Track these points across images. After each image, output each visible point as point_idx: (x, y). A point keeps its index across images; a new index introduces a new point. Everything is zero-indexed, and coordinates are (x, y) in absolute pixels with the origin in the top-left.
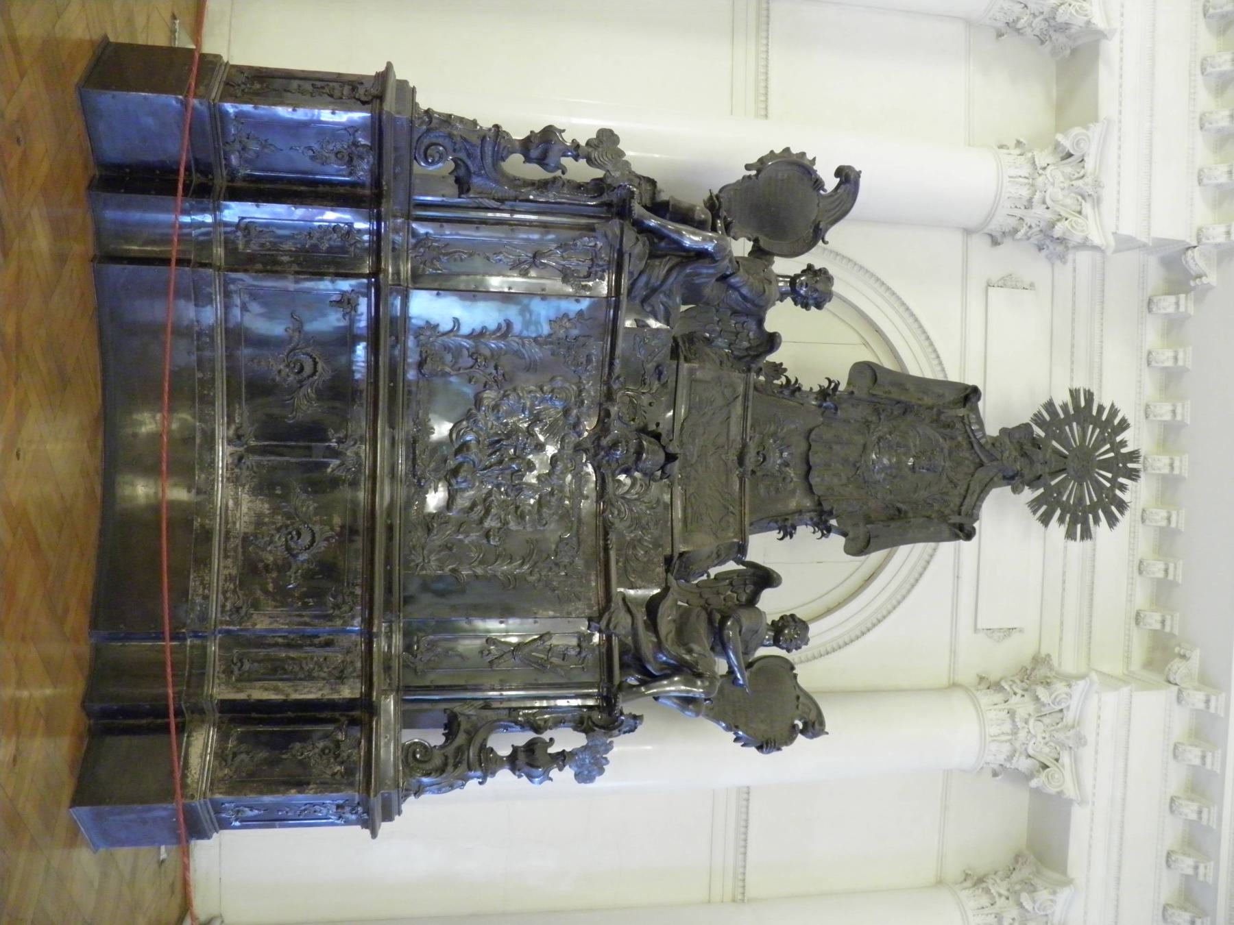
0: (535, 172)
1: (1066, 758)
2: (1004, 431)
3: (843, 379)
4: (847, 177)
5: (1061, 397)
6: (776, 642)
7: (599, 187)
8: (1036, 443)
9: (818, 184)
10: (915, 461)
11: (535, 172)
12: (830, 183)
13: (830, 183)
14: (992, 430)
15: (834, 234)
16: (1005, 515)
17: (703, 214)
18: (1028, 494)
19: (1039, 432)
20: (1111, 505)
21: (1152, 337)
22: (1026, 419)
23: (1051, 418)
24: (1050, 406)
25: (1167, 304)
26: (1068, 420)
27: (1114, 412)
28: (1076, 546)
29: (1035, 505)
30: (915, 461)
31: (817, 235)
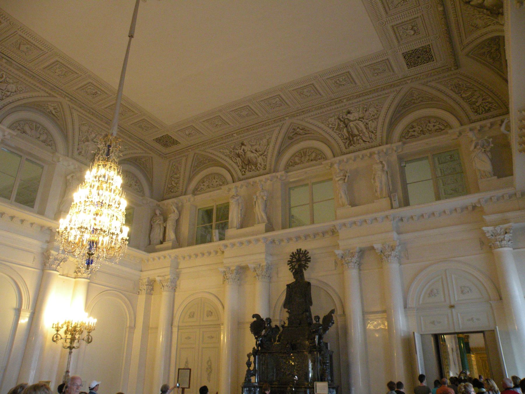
0: (253, 365)
2: (294, 278)
3: (286, 310)
4: (254, 316)
6: (319, 321)
7: (255, 357)
8: (295, 271)
9: (255, 321)
11: (253, 365)
12: (255, 319)
13: (255, 319)
14: (294, 280)
15: (262, 317)
20: (306, 253)
21: (283, 244)
22: (292, 274)
23: (292, 268)
24: (290, 269)
25: (277, 242)
26: (292, 265)
27: (291, 256)
29: (305, 269)
30: (299, 294)
31: (262, 320)
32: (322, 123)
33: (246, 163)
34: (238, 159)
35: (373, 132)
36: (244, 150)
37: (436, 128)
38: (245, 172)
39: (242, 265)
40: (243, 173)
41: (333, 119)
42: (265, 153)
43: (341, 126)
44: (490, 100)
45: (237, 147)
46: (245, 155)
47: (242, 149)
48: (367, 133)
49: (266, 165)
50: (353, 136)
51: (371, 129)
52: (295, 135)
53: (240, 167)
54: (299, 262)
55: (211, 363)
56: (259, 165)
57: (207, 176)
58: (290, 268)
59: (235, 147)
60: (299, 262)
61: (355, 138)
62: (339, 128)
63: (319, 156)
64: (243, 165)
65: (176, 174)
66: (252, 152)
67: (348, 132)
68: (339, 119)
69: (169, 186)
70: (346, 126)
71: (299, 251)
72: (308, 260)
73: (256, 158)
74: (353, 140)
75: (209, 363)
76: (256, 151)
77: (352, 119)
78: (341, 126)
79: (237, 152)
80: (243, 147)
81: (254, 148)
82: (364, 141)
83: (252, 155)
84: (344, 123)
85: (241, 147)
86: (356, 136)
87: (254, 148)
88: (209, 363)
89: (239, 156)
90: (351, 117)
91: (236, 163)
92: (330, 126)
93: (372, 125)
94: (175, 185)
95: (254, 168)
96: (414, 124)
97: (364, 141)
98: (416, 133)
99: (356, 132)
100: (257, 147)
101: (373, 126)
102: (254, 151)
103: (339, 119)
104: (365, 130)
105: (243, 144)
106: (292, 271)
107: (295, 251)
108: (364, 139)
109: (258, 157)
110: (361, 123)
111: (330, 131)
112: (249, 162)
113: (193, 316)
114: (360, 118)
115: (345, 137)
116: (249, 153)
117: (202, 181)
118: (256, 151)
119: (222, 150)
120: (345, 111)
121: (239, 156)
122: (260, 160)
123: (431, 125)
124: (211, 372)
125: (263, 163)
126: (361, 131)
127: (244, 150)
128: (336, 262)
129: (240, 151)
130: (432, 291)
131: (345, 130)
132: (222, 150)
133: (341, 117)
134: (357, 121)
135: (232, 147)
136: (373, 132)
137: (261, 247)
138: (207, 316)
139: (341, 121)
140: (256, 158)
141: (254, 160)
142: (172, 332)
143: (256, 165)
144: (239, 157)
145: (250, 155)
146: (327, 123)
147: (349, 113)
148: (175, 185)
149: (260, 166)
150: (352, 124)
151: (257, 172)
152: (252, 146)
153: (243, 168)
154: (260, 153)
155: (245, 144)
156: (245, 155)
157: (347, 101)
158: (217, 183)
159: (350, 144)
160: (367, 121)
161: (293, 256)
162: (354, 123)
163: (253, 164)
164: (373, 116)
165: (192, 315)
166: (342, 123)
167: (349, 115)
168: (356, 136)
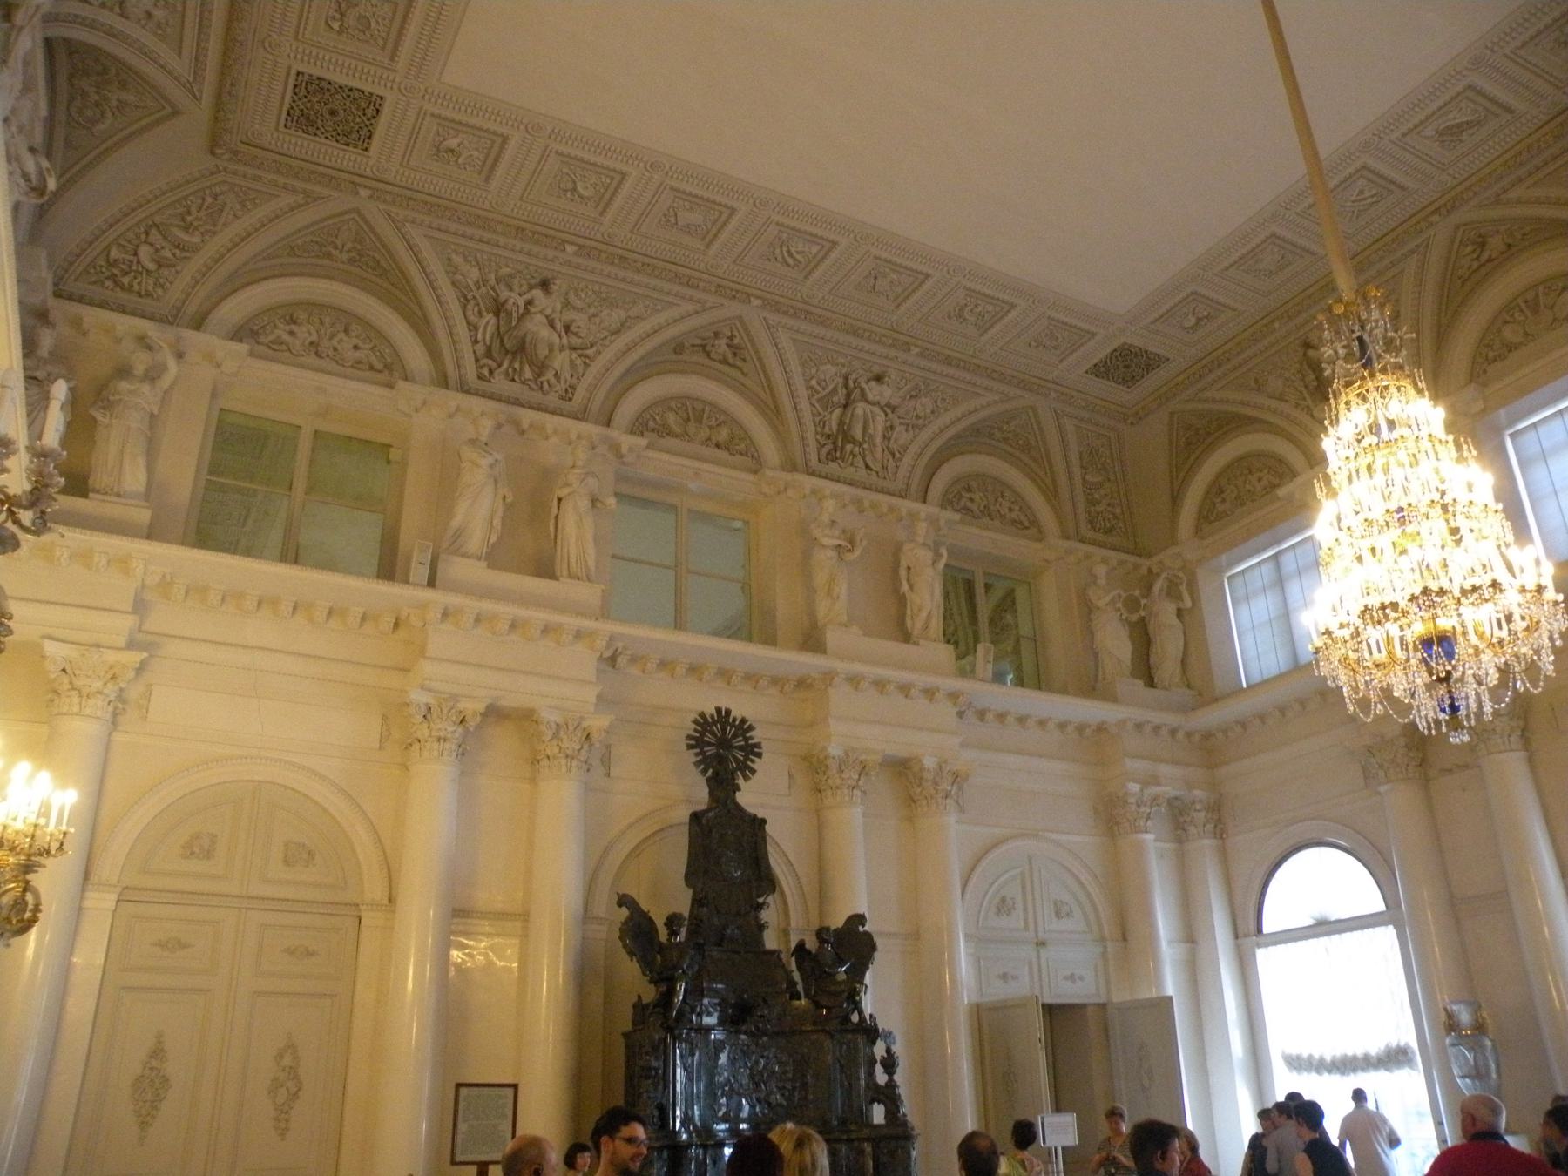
1: (863, 757)
5: (691, 757)
10: (727, 848)
16: (749, 796)
17: (663, 988)
18: (740, 781)
19: (710, 773)
20: (744, 727)
23: (704, 763)
28: (765, 749)
29: (746, 778)
30: (727, 848)
32: (803, 365)
33: (508, 344)
34: (490, 317)
35: (893, 455)
36: (529, 303)
37: (1014, 515)
38: (491, 372)
39: (503, 703)
40: (486, 372)
41: (833, 369)
42: (590, 352)
43: (835, 400)
44: (1118, 511)
45: (516, 281)
46: (520, 319)
47: (527, 297)
48: (879, 449)
49: (573, 388)
50: (848, 438)
51: (893, 445)
52: (722, 351)
53: (480, 349)
54: (722, 748)
55: (296, 1058)
56: (550, 375)
57: (315, 307)
58: (695, 759)
59: (512, 276)
60: (722, 748)
61: (849, 447)
62: (826, 403)
63: (737, 446)
64: (496, 345)
65: (187, 228)
66: (552, 325)
67: (841, 422)
68: (846, 379)
69: (114, 253)
70: (845, 406)
71: (723, 716)
72: (753, 750)
73: (551, 350)
74: (843, 448)
75: (287, 1061)
76: (567, 328)
77: (870, 397)
78: (835, 400)
79: (504, 294)
80: (537, 293)
81: (569, 315)
82: (867, 466)
83: (545, 332)
84: (848, 395)
85: (531, 288)
86: (854, 442)
87: (569, 315)
88: (287, 1061)
89: (498, 308)
90: (873, 391)
91: (473, 327)
92: (814, 382)
93: (901, 436)
94: (152, 266)
95: (528, 374)
96: (974, 484)
97: (867, 466)
98: (974, 507)
99: (858, 433)
100: (579, 319)
101: (901, 442)
102: (559, 326)
103: (846, 379)
104: (878, 440)
105: (545, 285)
106: (704, 772)
107: (710, 710)
108: (868, 459)
109: (561, 349)
110: (881, 418)
111: (803, 393)
112: (522, 349)
113: (209, 854)
114: (888, 405)
115: (827, 430)
116: (539, 318)
117: (290, 314)
118: (567, 328)
119: (458, 260)
120: (876, 370)
121: (498, 308)
122: (560, 361)
123: (1006, 504)
124: (295, 1096)
125: (566, 375)
126: (872, 437)
127: (529, 303)
128: (791, 776)
129: (515, 300)
130: (1003, 900)
131: (838, 412)
132: (458, 260)
133: (853, 376)
134: (876, 409)
135: (505, 271)
136: (893, 455)
137: (584, 661)
138: (286, 862)
139: (846, 386)
140: (551, 350)
141: (543, 352)
142: (80, 910)
143: (540, 368)
144: (497, 315)
145: (536, 327)
146: (814, 371)
147: (879, 379)
148: (152, 266)
149: (553, 380)
150: (860, 408)
151: (537, 397)
152: (567, 305)
153: (489, 353)
154: (577, 342)
155: (554, 288)
156: (520, 319)
157: (921, 355)
158: (358, 354)
159: (831, 457)
160: (897, 421)
161: (703, 723)
162: (868, 407)
163: (531, 364)
164: (918, 417)
165: (199, 848)
166: (842, 392)
167: (873, 383)
168: (854, 442)
